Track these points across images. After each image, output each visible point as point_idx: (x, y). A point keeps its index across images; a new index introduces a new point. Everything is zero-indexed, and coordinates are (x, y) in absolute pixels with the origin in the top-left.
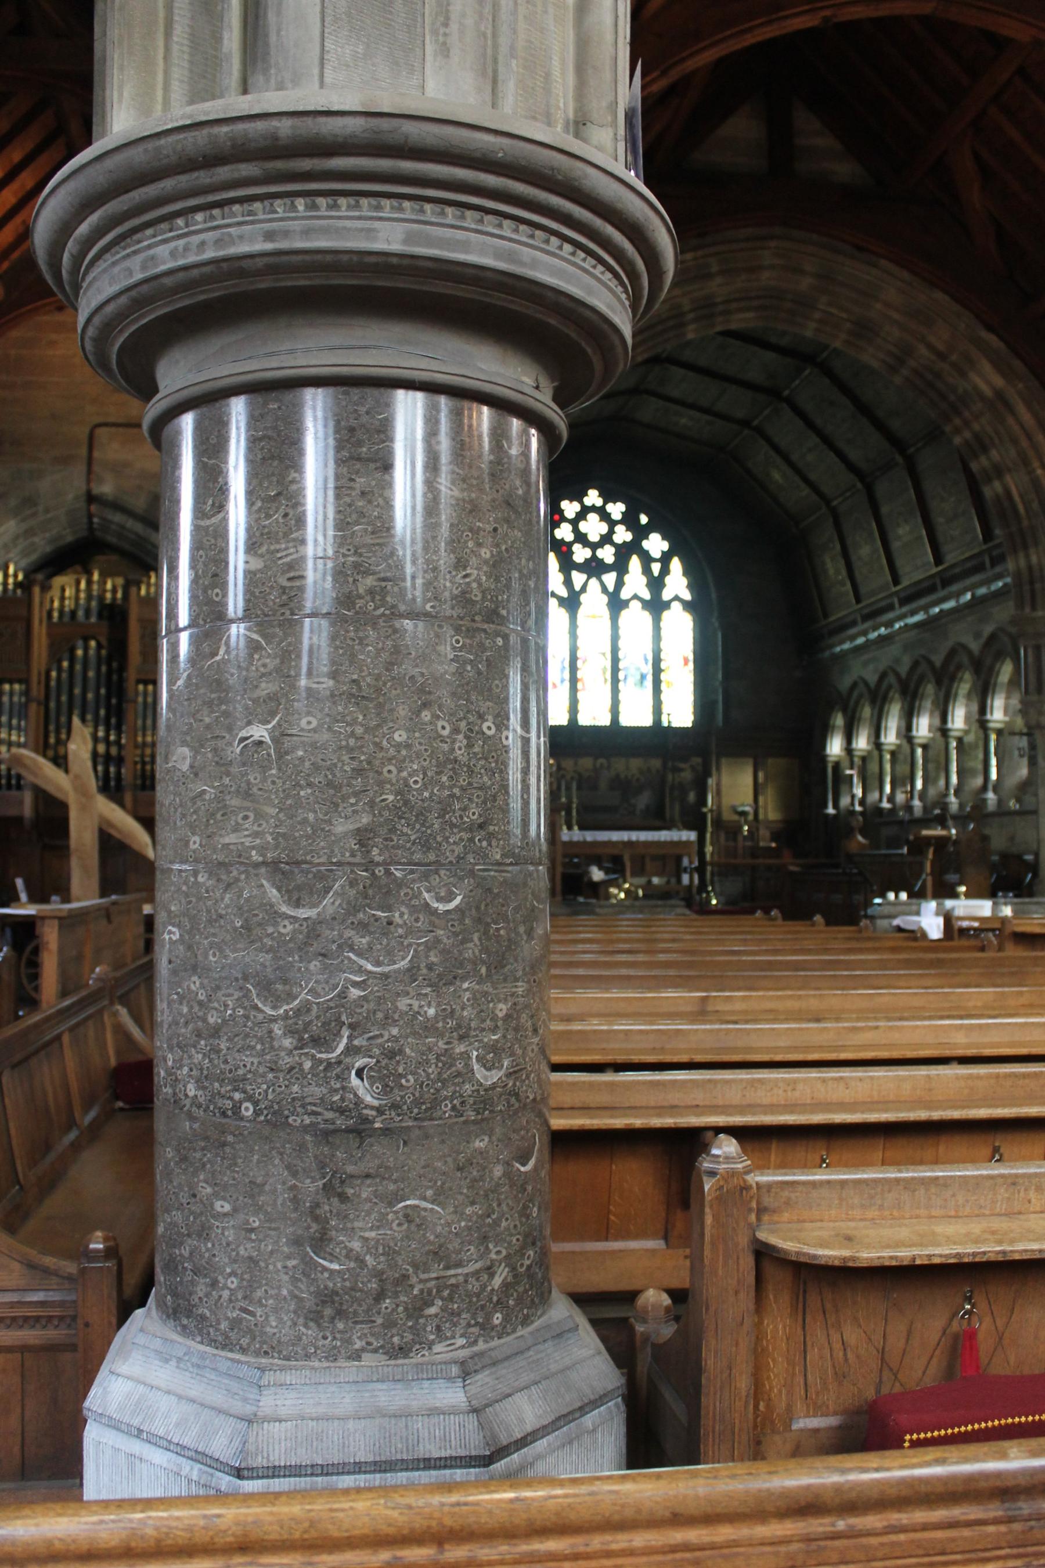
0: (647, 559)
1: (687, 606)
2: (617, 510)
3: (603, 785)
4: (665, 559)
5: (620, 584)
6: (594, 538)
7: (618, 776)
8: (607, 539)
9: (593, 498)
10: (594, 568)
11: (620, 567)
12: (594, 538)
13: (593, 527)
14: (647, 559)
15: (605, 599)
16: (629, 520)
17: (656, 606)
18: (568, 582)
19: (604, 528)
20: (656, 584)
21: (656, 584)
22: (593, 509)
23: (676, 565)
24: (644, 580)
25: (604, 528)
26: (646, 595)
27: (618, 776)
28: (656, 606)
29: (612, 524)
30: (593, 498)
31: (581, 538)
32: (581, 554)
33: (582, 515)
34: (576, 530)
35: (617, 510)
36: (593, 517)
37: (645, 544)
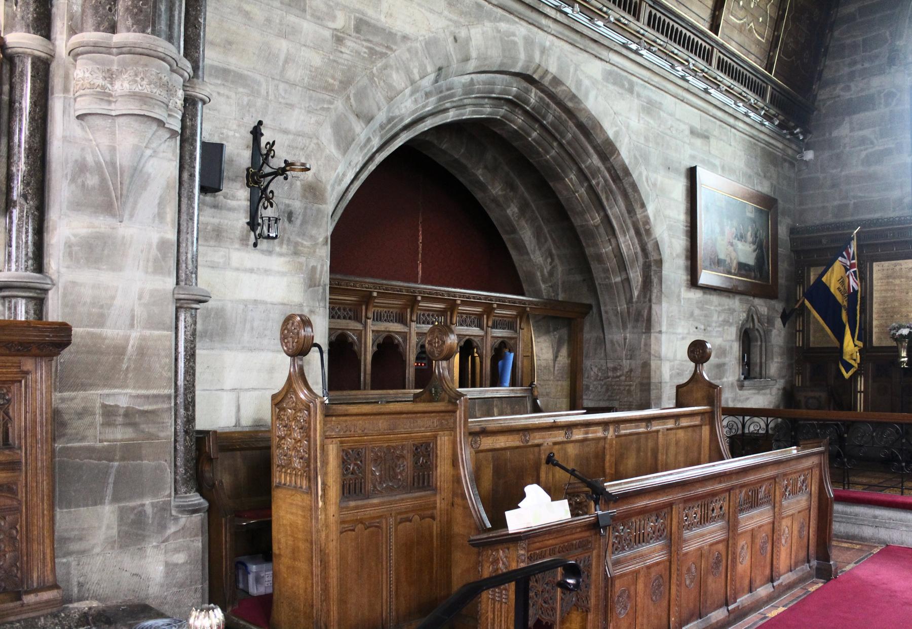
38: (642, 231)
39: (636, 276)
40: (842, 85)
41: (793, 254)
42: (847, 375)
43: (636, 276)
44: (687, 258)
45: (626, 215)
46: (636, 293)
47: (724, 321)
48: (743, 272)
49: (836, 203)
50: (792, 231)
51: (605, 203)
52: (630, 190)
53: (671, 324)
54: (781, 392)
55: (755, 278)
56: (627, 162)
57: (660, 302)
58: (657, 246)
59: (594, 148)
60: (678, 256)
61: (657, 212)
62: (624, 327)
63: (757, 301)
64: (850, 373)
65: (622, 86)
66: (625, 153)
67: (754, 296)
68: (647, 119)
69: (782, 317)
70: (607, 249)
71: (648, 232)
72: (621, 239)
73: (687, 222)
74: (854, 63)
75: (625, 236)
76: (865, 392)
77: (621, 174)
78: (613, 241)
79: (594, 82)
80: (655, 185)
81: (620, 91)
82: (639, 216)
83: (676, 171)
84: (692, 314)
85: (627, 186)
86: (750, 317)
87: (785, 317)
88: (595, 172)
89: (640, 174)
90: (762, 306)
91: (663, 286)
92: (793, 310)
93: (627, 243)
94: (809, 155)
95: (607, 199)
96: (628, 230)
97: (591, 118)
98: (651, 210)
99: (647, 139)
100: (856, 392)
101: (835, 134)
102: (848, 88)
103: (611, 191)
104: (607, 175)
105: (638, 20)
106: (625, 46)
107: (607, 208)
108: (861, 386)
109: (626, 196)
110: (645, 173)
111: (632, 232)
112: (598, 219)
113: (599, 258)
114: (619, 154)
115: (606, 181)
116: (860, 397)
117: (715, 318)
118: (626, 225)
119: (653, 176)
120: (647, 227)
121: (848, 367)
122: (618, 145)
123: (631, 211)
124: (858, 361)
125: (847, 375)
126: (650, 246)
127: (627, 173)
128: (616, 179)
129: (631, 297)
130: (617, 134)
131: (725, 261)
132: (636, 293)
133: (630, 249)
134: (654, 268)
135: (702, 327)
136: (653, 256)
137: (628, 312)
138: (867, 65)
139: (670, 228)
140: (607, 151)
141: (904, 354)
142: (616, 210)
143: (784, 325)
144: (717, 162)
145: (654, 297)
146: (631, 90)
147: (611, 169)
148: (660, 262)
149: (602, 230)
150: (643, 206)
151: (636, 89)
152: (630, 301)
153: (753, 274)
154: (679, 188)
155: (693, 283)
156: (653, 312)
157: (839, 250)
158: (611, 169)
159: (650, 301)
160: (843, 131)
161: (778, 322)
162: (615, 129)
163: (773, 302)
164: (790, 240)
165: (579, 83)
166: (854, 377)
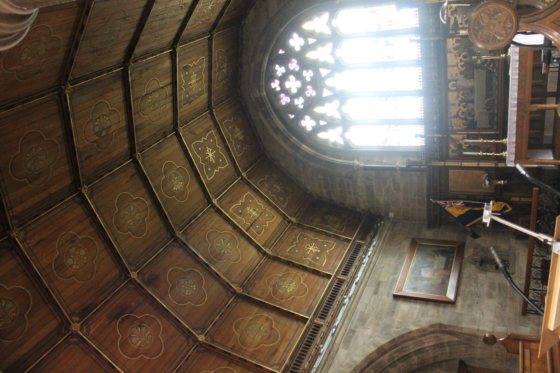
0: (306, 48)
1: (332, 16)
2: (280, 70)
3: (469, 83)
4: (305, 35)
5: (325, 65)
6: (299, 84)
7: (461, 73)
8: (298, 76)
9: (275, 85)
10: (317, 83)
11: (314, 66)
12: (299, 84)
13: (293, 84)
14: (306, 48)
15: (337, 75)
16: (284, 61)
17: (335, 38)
18: (329, 99)
19: (292, 78)
20: (321, 40)
21: (321, 40)
22: (281, 85)
23: (307, 26)
24: (320, 49)
25: (292, 78)
26: (329, 46)
27: (461, 73)
28: (335, 38)
29: (289, 72)
30: (275, 85)
31: (301, 92)
32: (310, 92)
33: (286, 92)
34: (297, 96)
35: (280, 70)
36: (288, 85)
37: (297, 49)
38: (423, 333)
39: (446, 338)
40: (359, 198)
41: (442, 227)
42: (510, 209)
43: (446, 338)
44: (439, 306)
45: (414, 341)
46: (456, 339)
47: (475, 283)
48: (449, 266)
49: (417, 204)
50: (430, 226)
51: (407, 353)
52: (402, 340)
53: (474, 321)
54: (518, 242)
55: (453, 258)
56: (388, 340)
57: (462, 328)
58: (431, 326)
59: (379, 357)
60: (438, 312)
61: (415, 324)
62: (473, 347)
63: (466, 256)
64: (508, 206)
65: (351, 337)
66: (383, 341)
67: (463, 258)
68: (368, 323)
69: (475, 238)
70: (431, 354)
71: (424, 330)
72: (426, 345)
73: (420, 303)
74: (350, 193)
75: (425, 343)
76: (520, 197)
77: (394, 344)
78: (427, 349)
79: (348, 355)
80: (400, 323)
81: (353, 338)
82: (416, 335)
83: (395, 306)
84: (470, 306)
85: (400, 341)
86: (474, 262)
87: (475, 236)
88: (391, 357)
89: (395, 332)
90: (469, 252)
91: (453, 325)
92: (472, 231)
93: (429, 342)
94: (391, 215)
95: (405, 351)
96: (422, 341)
97: (366, 359)
98: (413, 328)
99: (378, 325)
100: (520, 201)
101: (382, 203)
102: (361, 196)
103: (402, 349)
104: (394, 350)
105: (322, 326)
106: (333, 335)
107: (409, 352)
108: (517, 199)
109: (405, 341)
110: (394, 329)
111: (423, 338)
112: (415, 357)
113: (435, 357)
114: (384, 345)
115: (396, 352)
116: (523, 200)
117: (472, 289)
118: (420, 341)
119: (396, 324)
120: (422, 330)
121: (505, 208)
122: (380, 345)
123: (413, 339)
124: (502, 203)
125: (510, 209)
126: (433, 330)
127: (393, 340)
128: (396, 346)
129: (458, 341)
130: (374, 345)
131: (442, 279)
132: (456, 339)
133: (432, 341)
134: (443, 329)
135: (477, 299)
136: (437, 328)
137: (466, 344)
138: (351, 187)
139: (423, 315)
140: (381, 351)
141: (499, 182)
142: (411, 347)
143: (479, 236)
144: (392, 277)
145: (460, 331)
146: (353, 332)
147: (390, 349)
148: (440, 325)
149: (420, 355)
150: (410, 332)
151: (353, 328)
152: (460, 343)
153: (451, 259)
154: (404, 307)
155: (452, 303)
156: (466, 332)
157: (442, 209)
158: (390, 349)
159: (461, 333)
160: (382, 199)
161: (478, 241)
162: (371, 346)
163: (467, 244)
164: (434, 228)
165: (348, 365)
166: (511, 204)
